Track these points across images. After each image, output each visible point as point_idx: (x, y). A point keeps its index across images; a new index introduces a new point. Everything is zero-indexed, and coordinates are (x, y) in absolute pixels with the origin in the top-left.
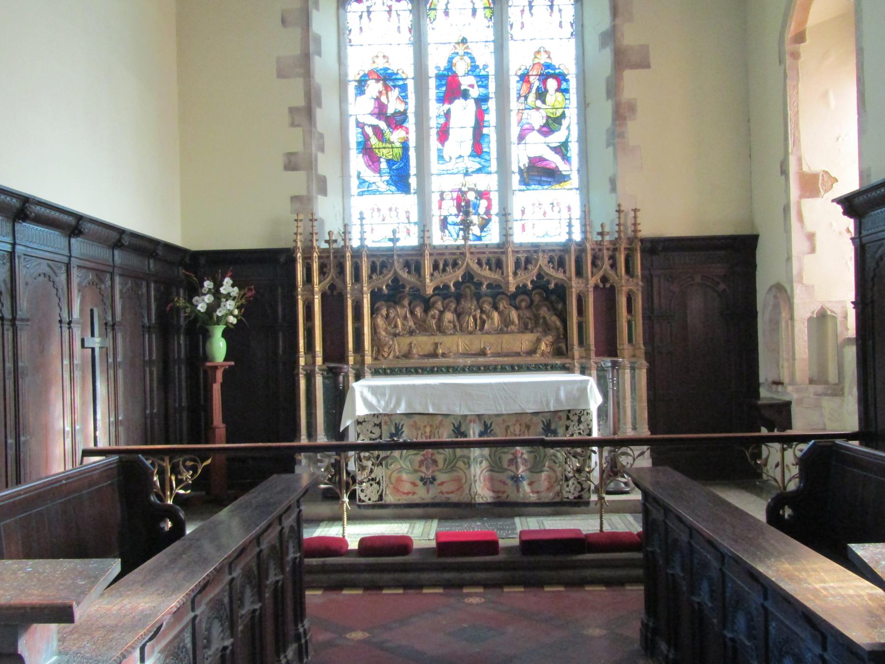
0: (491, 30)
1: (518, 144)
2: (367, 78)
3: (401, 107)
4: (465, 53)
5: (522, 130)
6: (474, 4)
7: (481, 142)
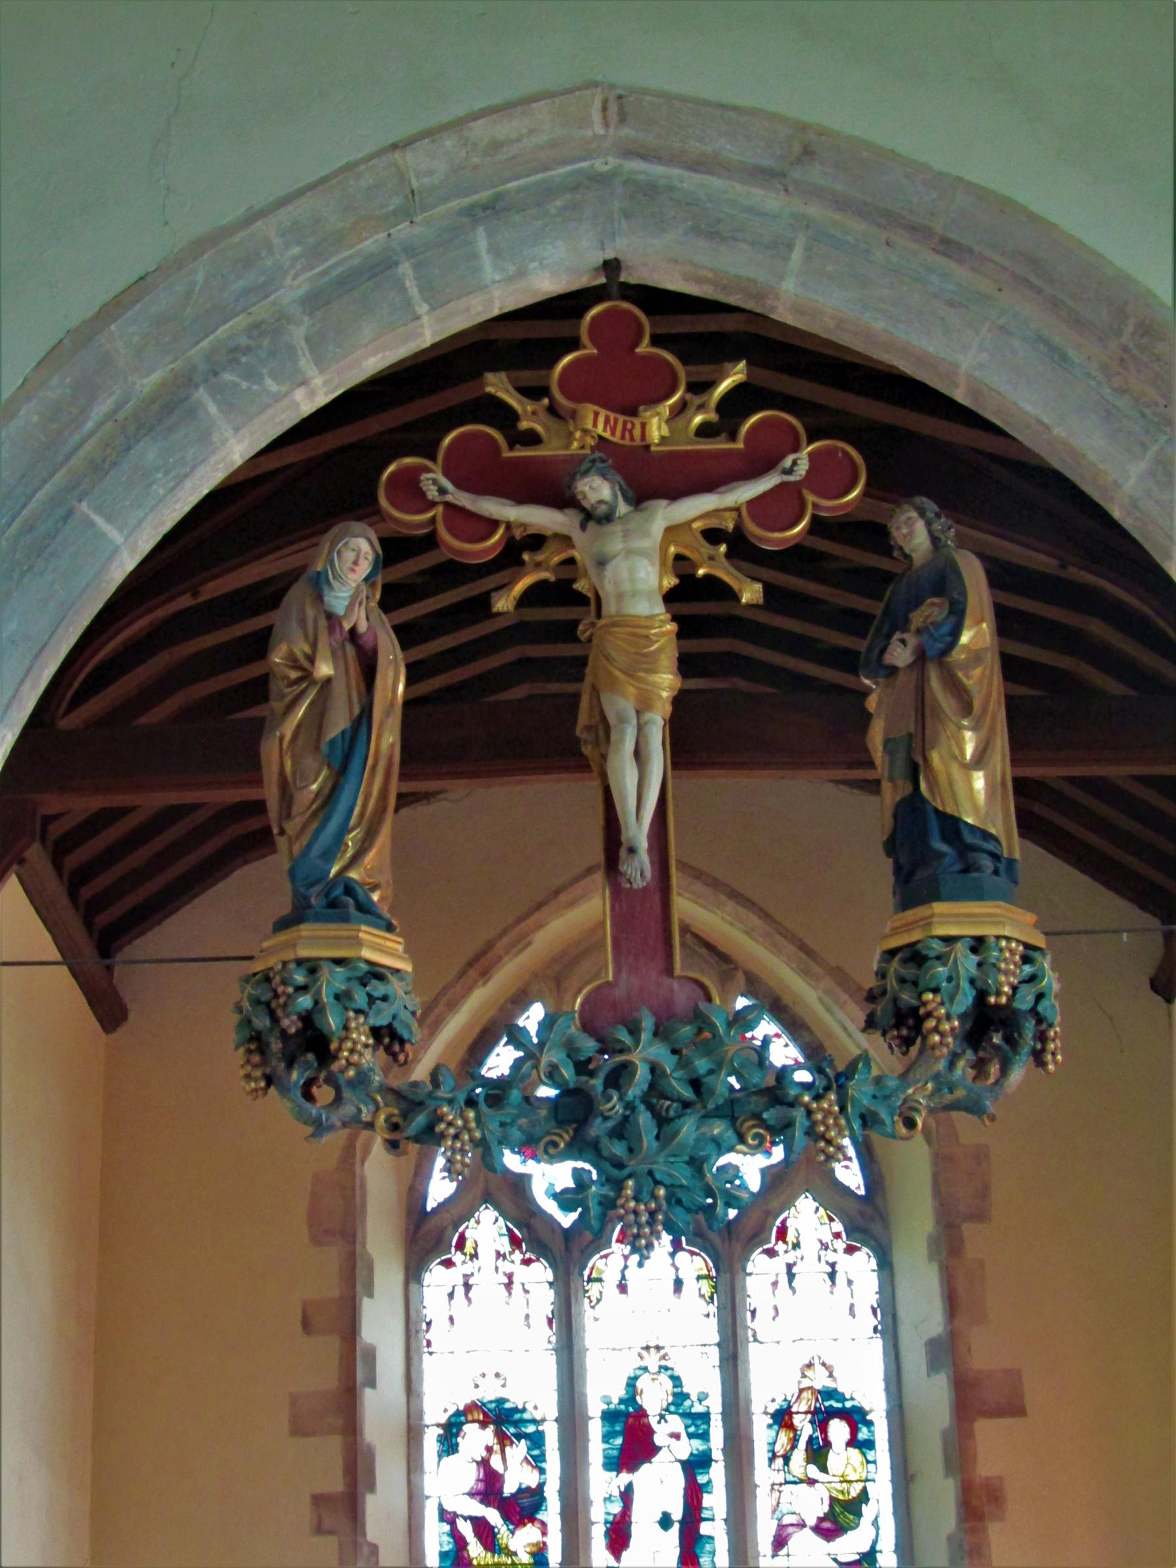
0: (713, 1322)
1: (773, 1556)
2: (463, 1418)
3: (531, 1479)
4: (660, 1367)
5: (781, 1527)
6: (677, 1269)
7: (698, 1551)
